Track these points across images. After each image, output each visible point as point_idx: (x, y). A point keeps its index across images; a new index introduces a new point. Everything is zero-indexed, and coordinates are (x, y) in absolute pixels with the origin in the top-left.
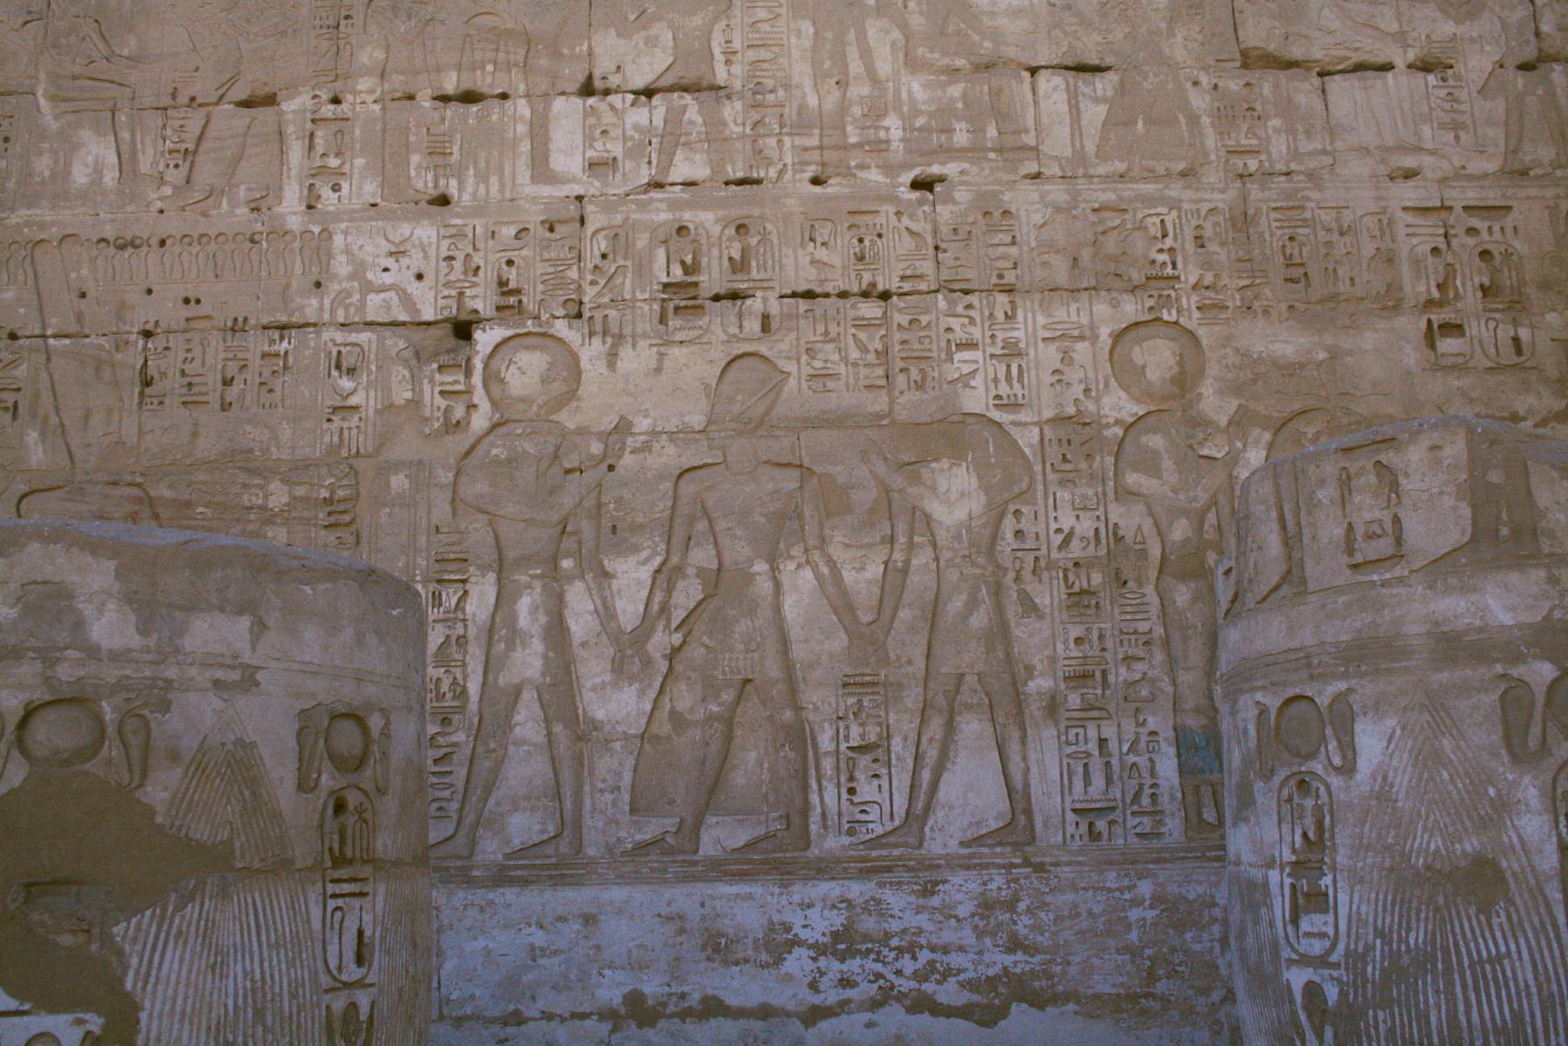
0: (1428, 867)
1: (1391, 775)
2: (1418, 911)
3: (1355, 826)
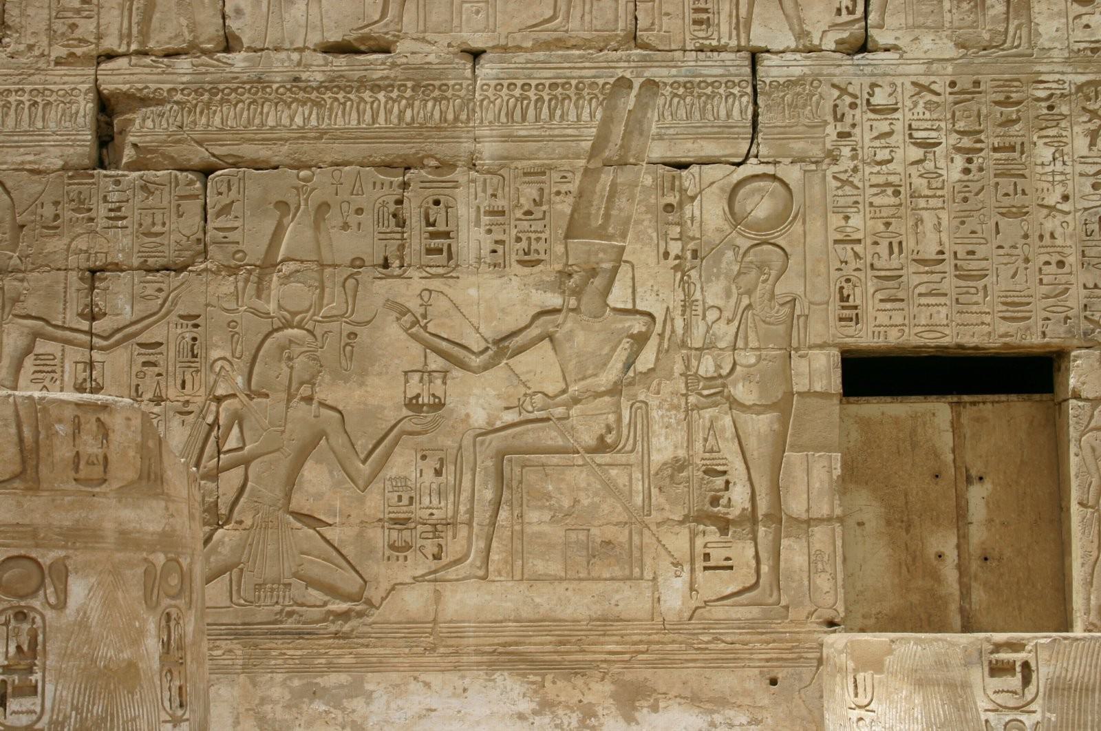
0: (105, 667)
1: (88, 612)
2: (100, 693)
3: (62, 642)
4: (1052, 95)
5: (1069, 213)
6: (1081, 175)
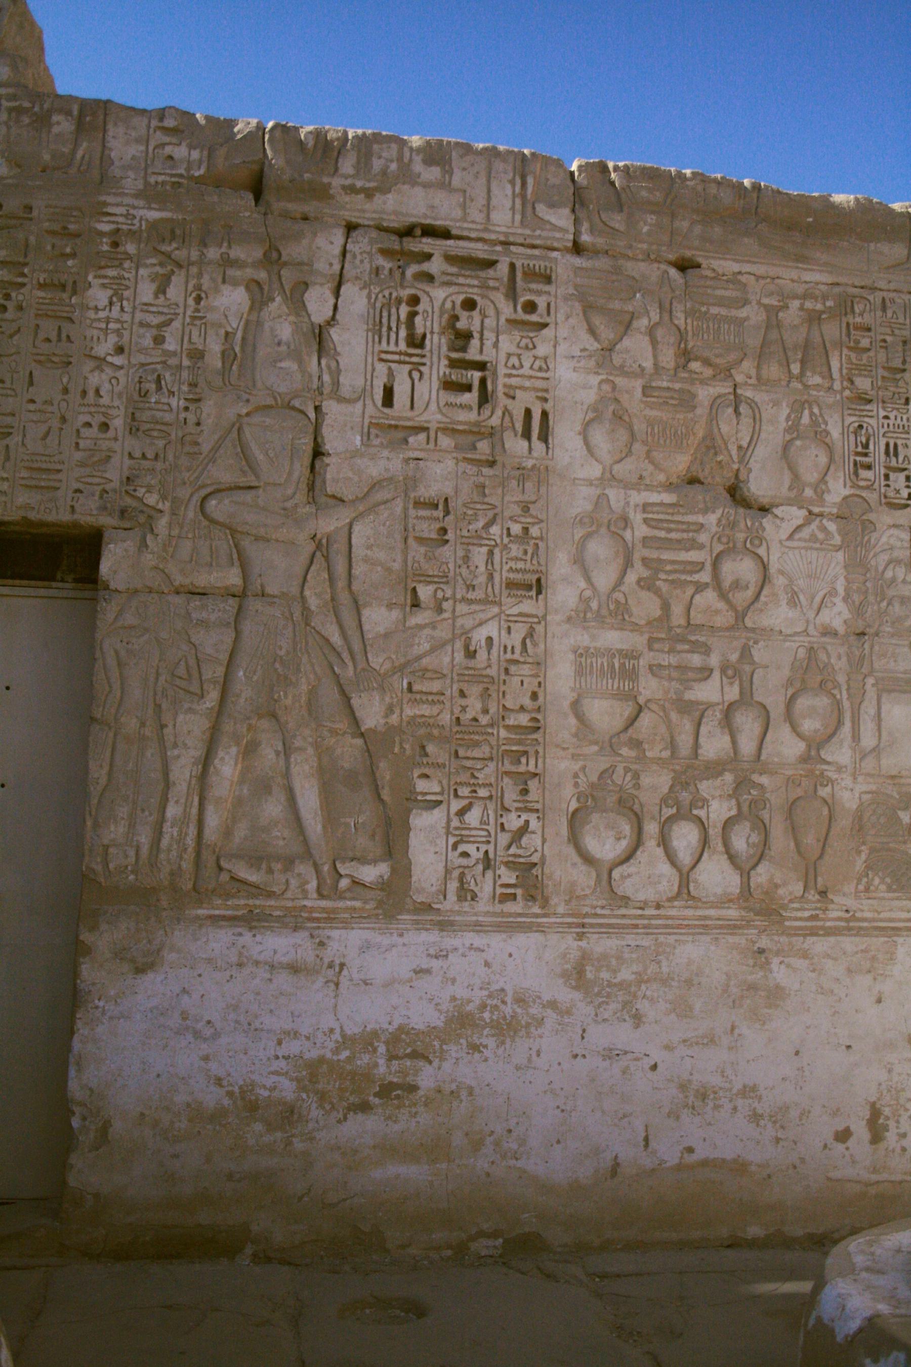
4: (118, 230)
5: (121, 368)
6: (141, 324)
